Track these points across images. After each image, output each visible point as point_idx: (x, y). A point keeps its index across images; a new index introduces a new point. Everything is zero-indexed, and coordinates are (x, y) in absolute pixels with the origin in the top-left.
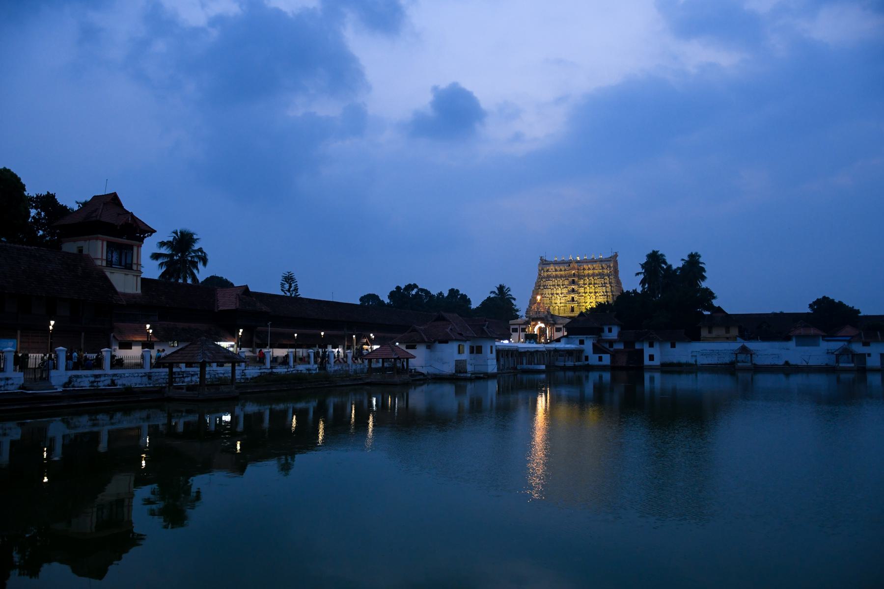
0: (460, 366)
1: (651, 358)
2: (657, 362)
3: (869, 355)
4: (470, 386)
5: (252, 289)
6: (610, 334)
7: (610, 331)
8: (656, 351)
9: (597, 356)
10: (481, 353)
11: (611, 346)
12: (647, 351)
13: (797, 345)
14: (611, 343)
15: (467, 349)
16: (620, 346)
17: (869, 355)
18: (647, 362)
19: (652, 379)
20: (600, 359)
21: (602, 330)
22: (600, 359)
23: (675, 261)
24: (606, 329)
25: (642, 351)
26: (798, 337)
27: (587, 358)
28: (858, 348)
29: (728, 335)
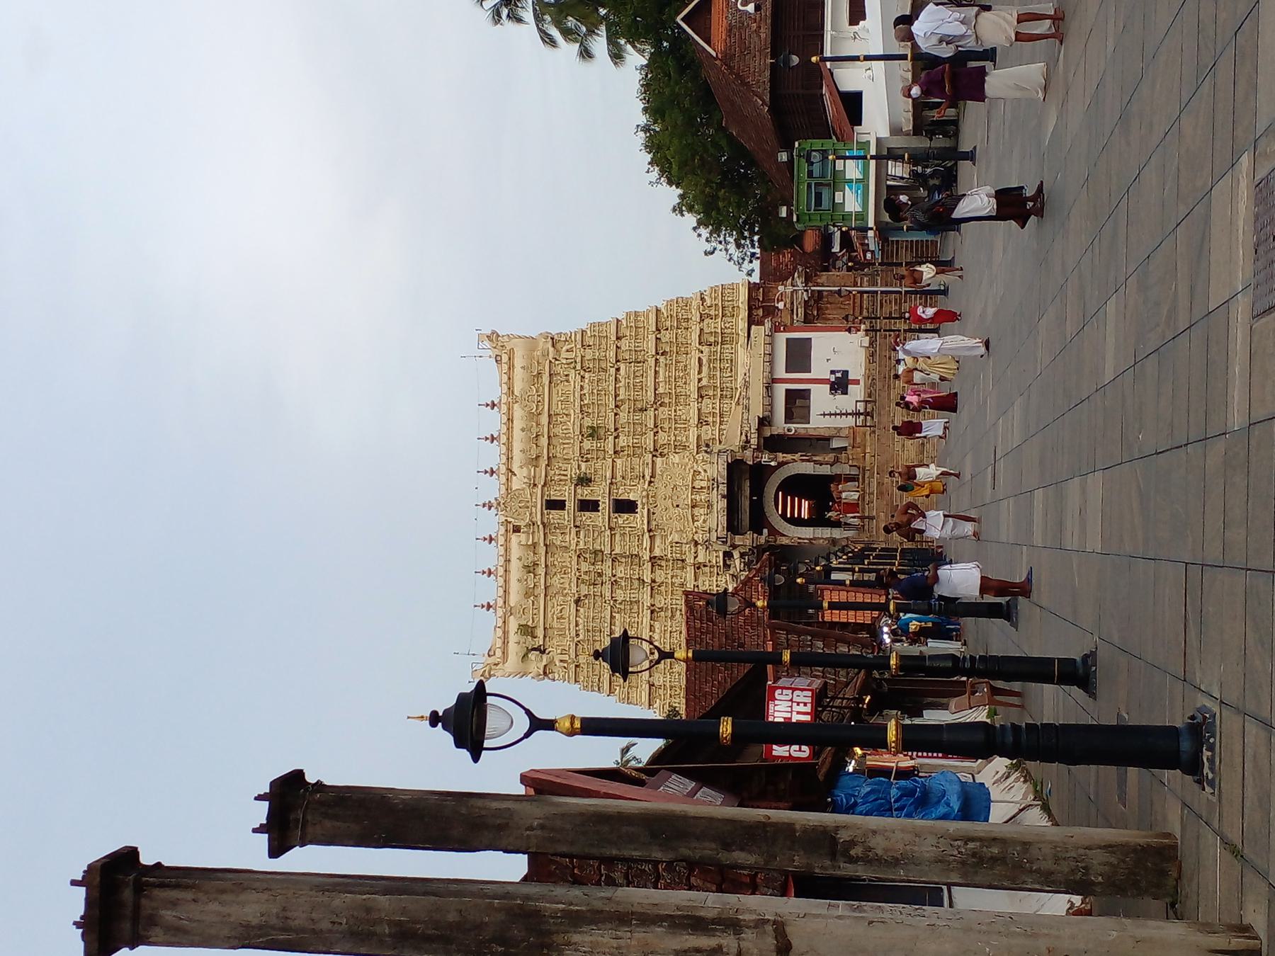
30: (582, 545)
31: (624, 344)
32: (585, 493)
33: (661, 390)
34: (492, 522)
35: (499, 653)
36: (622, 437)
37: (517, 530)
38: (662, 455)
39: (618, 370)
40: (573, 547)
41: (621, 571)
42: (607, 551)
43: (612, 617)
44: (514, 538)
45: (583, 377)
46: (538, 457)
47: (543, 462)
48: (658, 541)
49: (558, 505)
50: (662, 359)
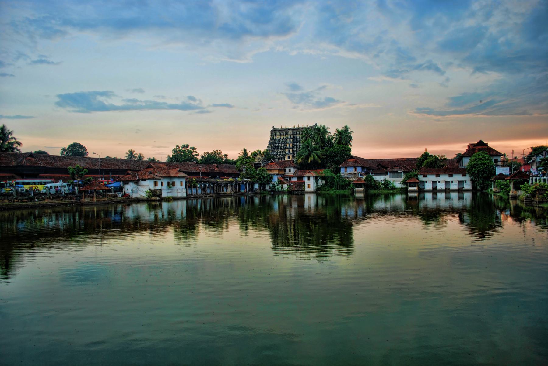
0: (153, 193)
1: (309, 187)
4: (165, 205)
7: (290, 170)
11: (290, 179)
14: (290, 178)
15: (165, 184)
16: (295, 180)
18: (307, 189)
19: (309, 198)
21: (285, 170)
24: (287, 169)
25: (304, 183)
26: (390, 172)
28: (421, 178)
29: (356, 172)
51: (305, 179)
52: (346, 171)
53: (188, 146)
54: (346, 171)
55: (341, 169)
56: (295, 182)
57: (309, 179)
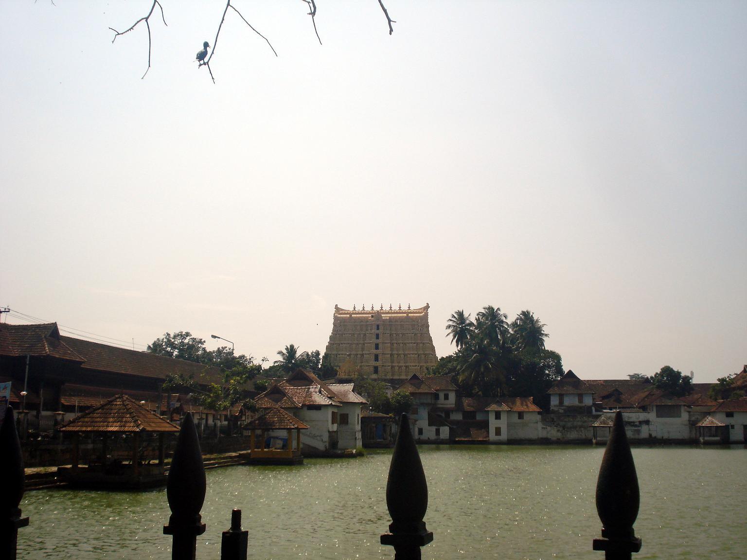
1: (498, 431)
2: (504, 436)
3: (733, 427)
5: (64, 331)
6: (446, 402)
7: (446, 397)
8: (503, 423)
9: (434, 428)
10: (347, 423)
12: (493, 423)
13: (658, 416)
14: (448, 412)
16: (457, 417)
17: (733, 427)
18: (492, 436)
20: (438, 432)
21: (436, 396)
22: (438, 432)
23: (511, 315)
27: (421, 431)
29: (580, 405)
30: (367, 334)
31: (421, 345)
32: (380, 336)
33: (409, 356)
34: (377, 308)
35: (341, 312)
36: (396, 345)
37: (372, 316)
38: (391, 356)
39: (415, 343)
40: (367, 332)
41: (360, 345)
42: (366, 342)
43: (348, 343)
44: (370, 315)
45: (412, 333)
46: (391, 321)
47: (391, 323)
48: (368, 356)
49: (378, 329)
50: (417, 355)
51: (492, 418)
52: (561, 402)
53: (188, 334)
54: (561, 402)
55: (552, 398)
56: (457, 422)
57: (498, 416)
